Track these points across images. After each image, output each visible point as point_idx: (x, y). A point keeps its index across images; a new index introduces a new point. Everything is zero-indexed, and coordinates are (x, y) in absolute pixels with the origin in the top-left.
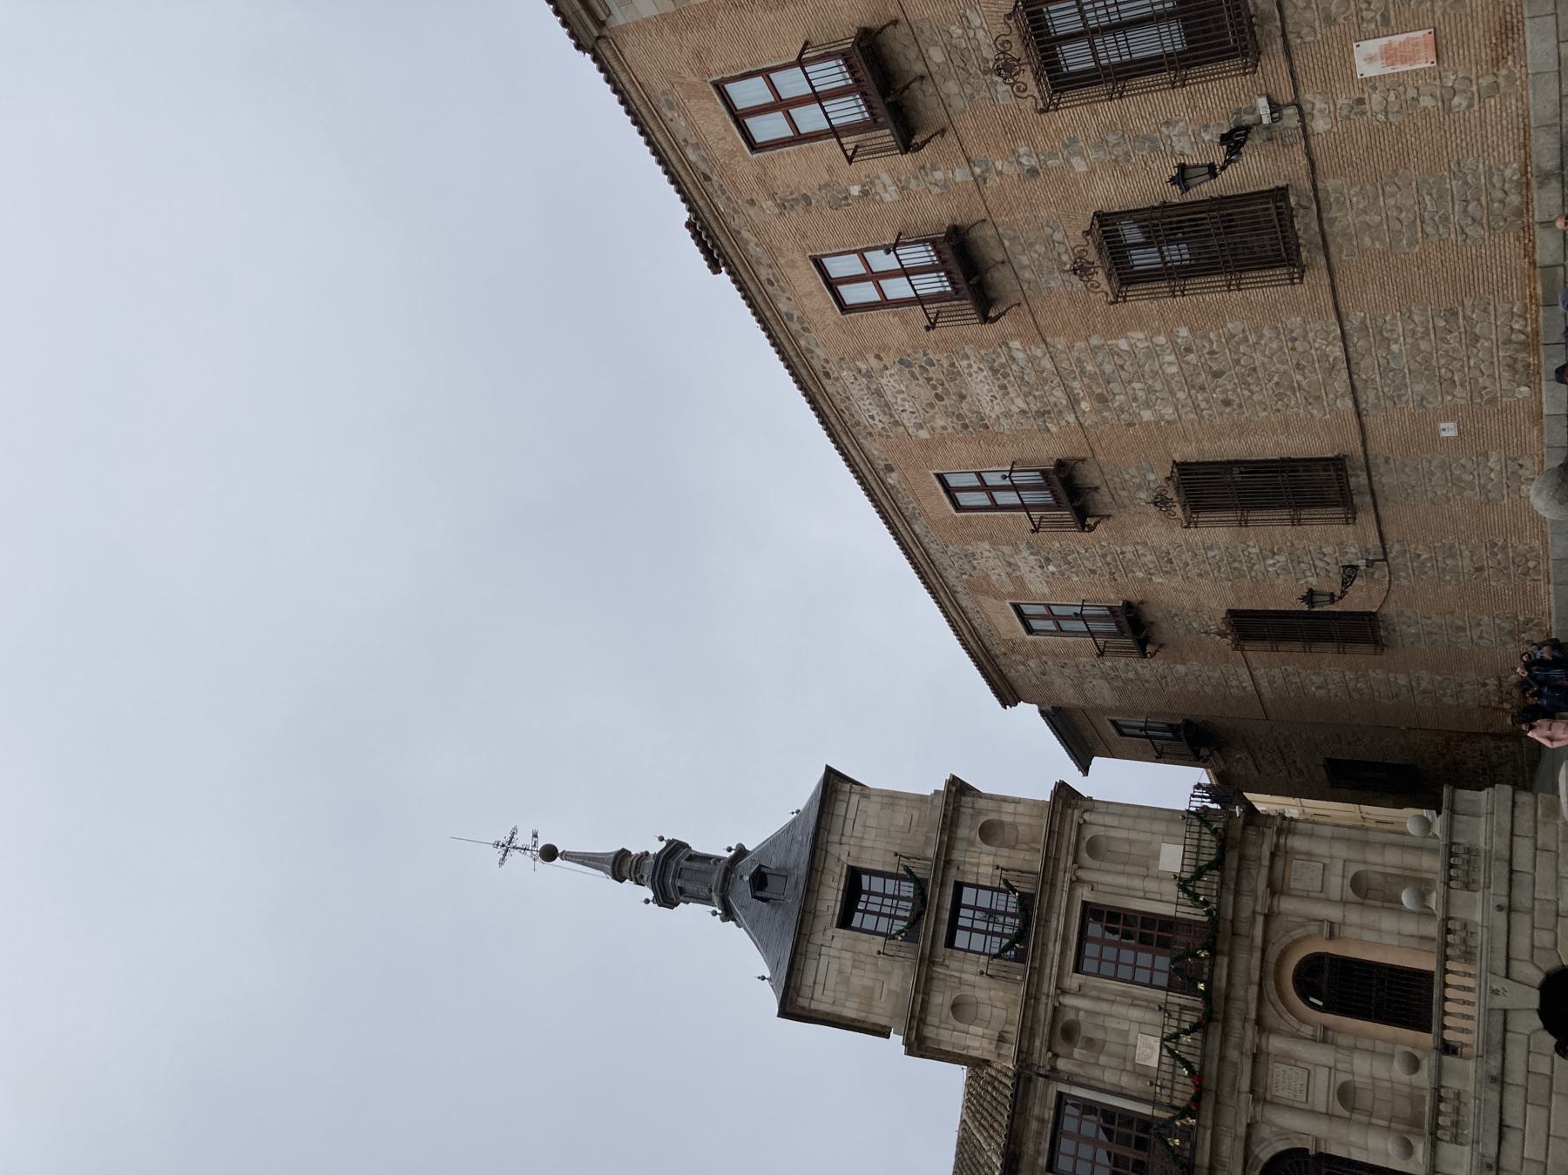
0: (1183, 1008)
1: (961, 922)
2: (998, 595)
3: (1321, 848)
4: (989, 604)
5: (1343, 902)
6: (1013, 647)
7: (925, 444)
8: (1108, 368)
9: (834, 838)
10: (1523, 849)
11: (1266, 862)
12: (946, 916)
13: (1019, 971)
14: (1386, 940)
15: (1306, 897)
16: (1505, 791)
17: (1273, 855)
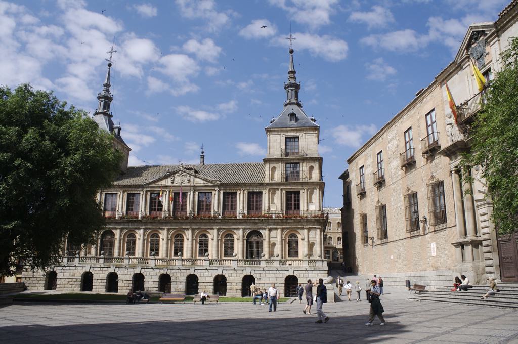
0: (283, 214)
1: (292, 165)
2: (365, 162)
3: (318, 236)
4: (363, 160)
5: (308, 241)
6: (357, 164)
7: (386, 149)
8: (398, 192)
9: (305, 132)
10: (317, 272)
11: (314, 226)
12: (292, 162)
13: (284, 181)
14: (303, 249)
15: (308, 235)
16: (327, 269)
17: (315, 228)
